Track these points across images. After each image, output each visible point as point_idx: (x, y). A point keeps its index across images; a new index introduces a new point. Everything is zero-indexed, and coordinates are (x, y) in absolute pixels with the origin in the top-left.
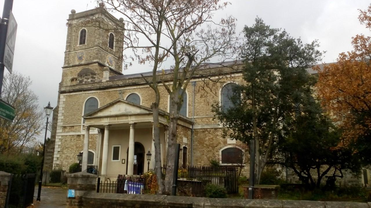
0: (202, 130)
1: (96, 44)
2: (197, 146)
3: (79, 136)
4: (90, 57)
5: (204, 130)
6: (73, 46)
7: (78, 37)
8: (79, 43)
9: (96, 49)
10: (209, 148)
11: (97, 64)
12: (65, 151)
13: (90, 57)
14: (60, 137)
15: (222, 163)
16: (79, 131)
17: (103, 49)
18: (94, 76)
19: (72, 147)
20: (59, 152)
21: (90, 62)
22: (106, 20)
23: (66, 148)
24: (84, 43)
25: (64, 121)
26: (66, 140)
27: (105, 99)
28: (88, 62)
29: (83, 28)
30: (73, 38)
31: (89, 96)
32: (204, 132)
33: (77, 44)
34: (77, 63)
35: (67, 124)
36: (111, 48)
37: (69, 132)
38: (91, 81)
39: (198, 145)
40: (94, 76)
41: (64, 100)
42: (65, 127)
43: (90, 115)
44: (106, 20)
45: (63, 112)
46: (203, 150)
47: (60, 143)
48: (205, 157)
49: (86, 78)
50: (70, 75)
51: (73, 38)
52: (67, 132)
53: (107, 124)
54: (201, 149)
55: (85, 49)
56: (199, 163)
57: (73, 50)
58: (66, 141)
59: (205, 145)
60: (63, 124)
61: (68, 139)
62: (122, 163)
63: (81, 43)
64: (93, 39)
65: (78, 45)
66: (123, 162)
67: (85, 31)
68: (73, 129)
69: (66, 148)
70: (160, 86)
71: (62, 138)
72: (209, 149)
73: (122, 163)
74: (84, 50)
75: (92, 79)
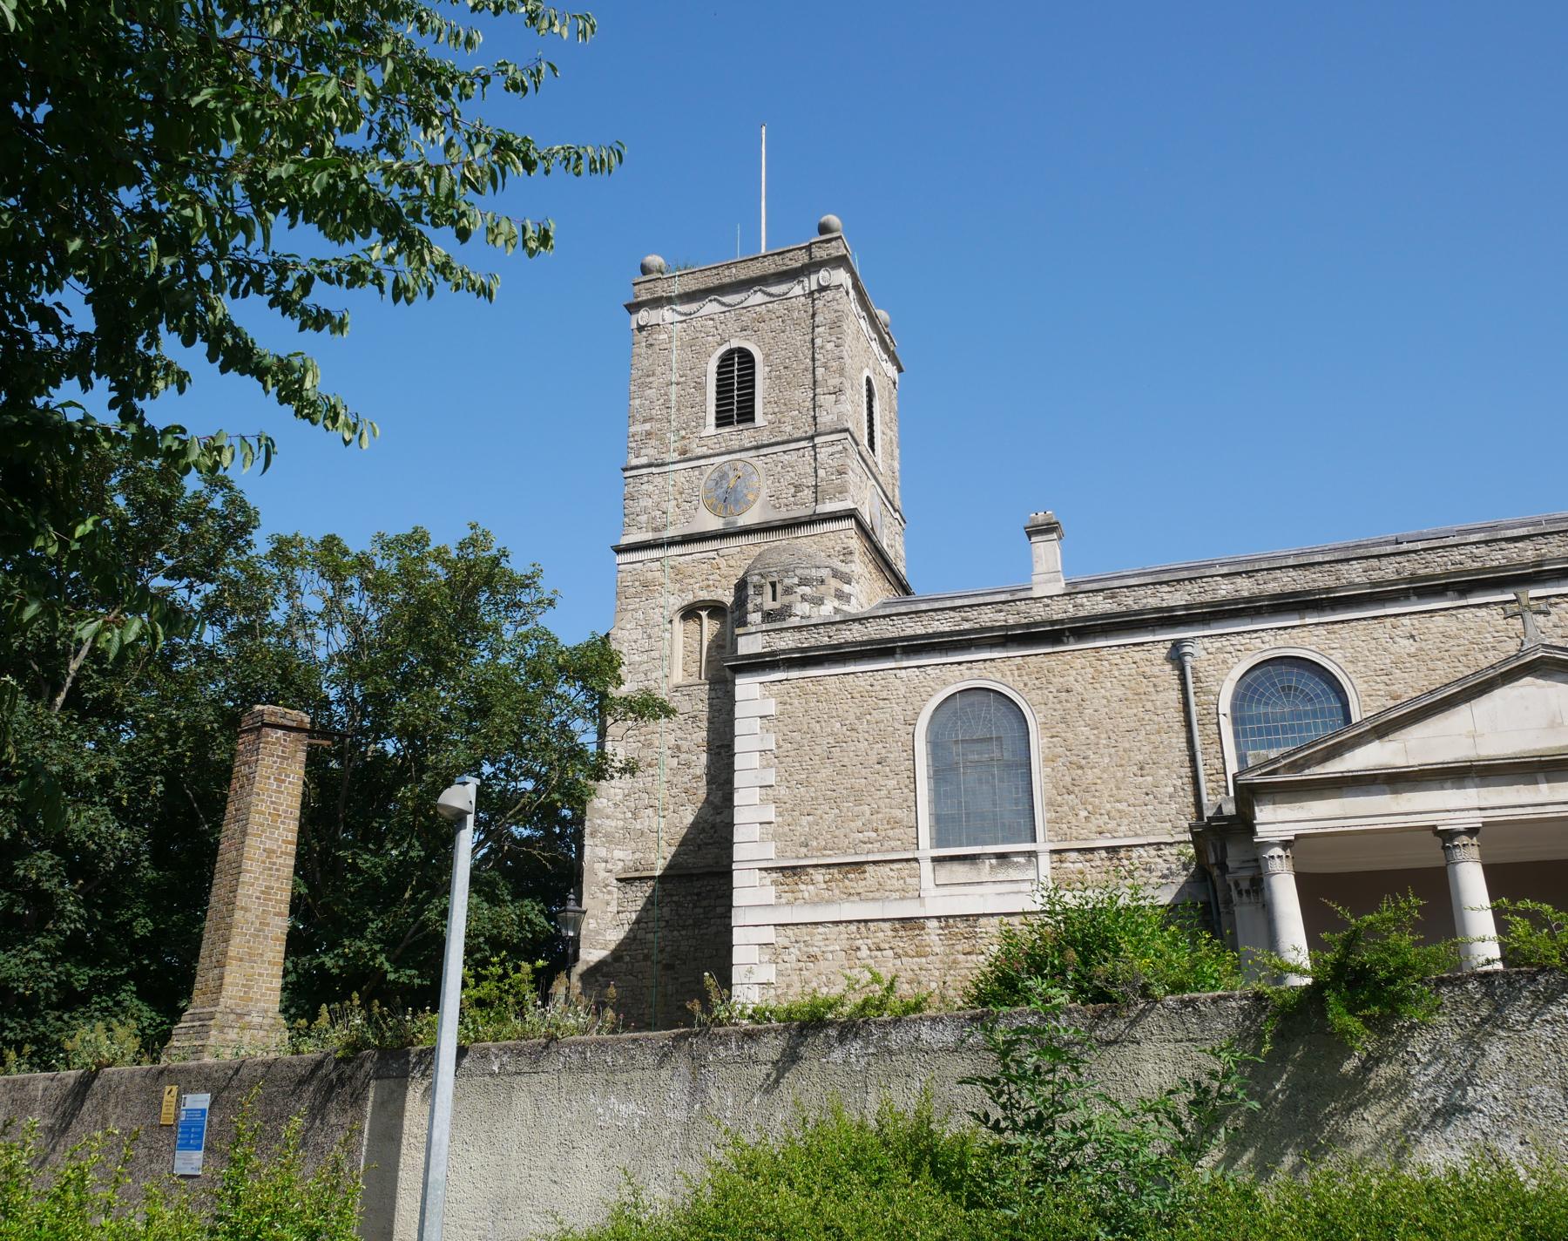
3: (909, 923)
4: (798, 488)
7: (700, 386)
8: (711, 418)
9: (832, 443)
11: (851, 523)
13: (798, 488)
14: (769, 935)
18: (846, 588)
24: (747, 415)
25: (775, 837)
26: (813, 950)
27: (1075, 699)
29: (735, 344)
30: (673, 397)
31: (945, 683)
33: (700, 421)
34: (714, 523)
35: (804, 850)
37: (829, 902)
38: (837, 610)
40: (846, 588)
41: (771, 707)
45: (771, 777)
49: (804, 598)
50: (670, 586)
51: (673, 397)
53: (1475, 820)
55: (757, 448)
57: (675, 456)
58: (812, 958)
60: (781, 854)
61: (837, 941)
63: (723, 420)
65: (711, 429)
67: (746, 357)
68: (854, 882)
70: (1479, 606)
71: (784, 942)
74: (752, 453)
75: (836, 603)
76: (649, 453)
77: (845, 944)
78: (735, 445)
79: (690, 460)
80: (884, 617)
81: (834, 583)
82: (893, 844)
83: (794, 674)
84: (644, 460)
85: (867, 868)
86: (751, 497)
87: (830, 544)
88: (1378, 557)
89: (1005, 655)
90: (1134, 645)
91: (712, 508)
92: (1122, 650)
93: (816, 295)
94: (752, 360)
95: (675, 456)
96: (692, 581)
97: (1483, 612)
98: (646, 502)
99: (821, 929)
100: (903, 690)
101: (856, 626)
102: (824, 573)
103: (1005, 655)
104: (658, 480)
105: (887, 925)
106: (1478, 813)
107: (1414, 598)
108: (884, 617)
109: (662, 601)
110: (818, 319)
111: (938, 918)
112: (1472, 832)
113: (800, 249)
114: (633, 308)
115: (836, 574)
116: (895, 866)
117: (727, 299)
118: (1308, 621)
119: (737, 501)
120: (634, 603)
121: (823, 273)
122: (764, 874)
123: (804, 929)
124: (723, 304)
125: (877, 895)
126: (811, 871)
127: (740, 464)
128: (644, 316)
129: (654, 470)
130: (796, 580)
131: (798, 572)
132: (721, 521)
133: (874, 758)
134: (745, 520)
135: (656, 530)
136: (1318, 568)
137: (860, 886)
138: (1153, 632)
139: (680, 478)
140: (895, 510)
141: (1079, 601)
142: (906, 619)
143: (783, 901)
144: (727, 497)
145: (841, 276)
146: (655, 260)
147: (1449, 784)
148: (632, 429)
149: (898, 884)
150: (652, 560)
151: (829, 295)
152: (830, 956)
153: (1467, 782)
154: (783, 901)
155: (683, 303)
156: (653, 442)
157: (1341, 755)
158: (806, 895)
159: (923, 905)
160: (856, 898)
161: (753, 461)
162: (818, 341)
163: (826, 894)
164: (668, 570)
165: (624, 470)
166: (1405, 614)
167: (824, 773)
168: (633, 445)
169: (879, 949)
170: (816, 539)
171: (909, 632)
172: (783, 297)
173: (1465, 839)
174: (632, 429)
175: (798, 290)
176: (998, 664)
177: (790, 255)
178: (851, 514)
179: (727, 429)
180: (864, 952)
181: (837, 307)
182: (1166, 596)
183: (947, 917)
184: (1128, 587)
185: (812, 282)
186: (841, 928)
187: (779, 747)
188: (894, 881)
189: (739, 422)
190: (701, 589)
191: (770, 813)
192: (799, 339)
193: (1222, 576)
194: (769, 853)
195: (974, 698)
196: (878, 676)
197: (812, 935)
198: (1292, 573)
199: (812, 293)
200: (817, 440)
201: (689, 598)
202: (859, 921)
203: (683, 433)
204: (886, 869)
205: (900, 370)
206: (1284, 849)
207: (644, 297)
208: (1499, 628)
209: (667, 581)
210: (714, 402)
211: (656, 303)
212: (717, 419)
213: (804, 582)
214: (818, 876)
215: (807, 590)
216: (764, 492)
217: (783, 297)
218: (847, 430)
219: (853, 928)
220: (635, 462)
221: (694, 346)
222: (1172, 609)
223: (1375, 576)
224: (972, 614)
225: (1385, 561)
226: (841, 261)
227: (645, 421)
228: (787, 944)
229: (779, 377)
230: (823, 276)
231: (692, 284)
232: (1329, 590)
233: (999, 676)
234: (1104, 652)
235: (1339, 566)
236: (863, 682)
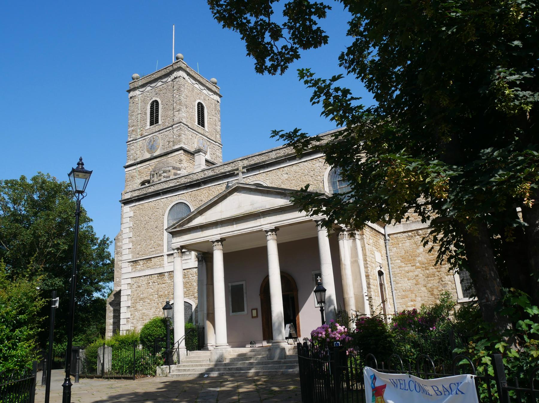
0: (406, 234)
1: (176, 120)
2: (400, 267)
3: (161, 274)
4: (169, 142)
5: (410, 234)
6: (139, 130)
7: (146, 114)
8: (148, 123)
10: (428, 269)
11: (182, 151)
12: (139, 306)
13: (169, 142)
14: (129, 281)
15: (464, 297)
16: (161, 266)
17: (189, 127)
19: (152, 297)
20: (128, 307)
21: (169, 150)
22: (189, 81)
23: (142, 299)
24: (157, 122)
25: (132, 252)
28: (165, 151)
29: (154, 99)
31: (172, 202)
32: (412, 237)
34: (148, 156)
36: (202, 126)
37: (143, 270)
39: (404, 265)
41: (132, 214)
42: (135, 262)
43: (180, 226)
44: (189, 81)
45: (131, 235)
46: (416, 273)
47: (129, 292)
48: (424, 289)
50: (138, 177)
51: (139, 118)
52: (139, 271)
53: (218, 237)
54: (411, 274)
55: (159, 131)
56: (412, 303)
58: (139, 287)
59: (418, 264)
60: (133, 257)
62: (253, 317)
63: (152, 124)
64: (170, 113)
65: (148, 126)
66: (254, 312)
68: (150, 264)
69: (142, 299)
72: (428, 272)
73: (253, 317)
74: (158, 133)
76: (133, 136)
77: (146, 282)
78: (154, 131)
79: (143, 137)
80: (159, 183)
81: (173, 171)
82: (158, 251)
83: (137, 203)
84: (132, 139)
85: (152, 259)
86: (157, 147)
87: (176, 159)
88: (279, 149)
89: (186, 192)
90: (218, 184)
91: (148, 151)
92: (215, 186)
93: (174, 80)
94: (158, 104)
95: (139, 136)
96: (143, 174)
97: (305, 164)
98: (132, 152)
99: (141, 278)
100: (162, 205)
101: (152, 187)
102: (170, 168)
103: (186, 192)
104: (135, 144)
105: (156, 275)
106: (219, 235)
107: (288, 161)
108: (159, 183)
109: (136, 182)
110: (175, 88)
111: (168, 272)
112: (217, 241)
113: (170, 66)
114: (129, 91)
115: (174, 168)
116: (159, 258)
117: (152, 85)
118: (261, 172)
119: (154, 148)
120: (129, 183)
121: (175, 73)
122: (129, 263)
123: (138, 279)
124: (151, 87)
125: (154, 267)
126: (139, 261)
127: (155, 137)
128: (132, 94)
129: (134, 141)
130: (162, 172)
131: (163, 169)
132: (150, 155)
133: (155, 226)
134: (155, 154)
135: (135, 160)
136: (264, 155)
137: (150, 265)
138: (223, 180)
139: (140, 143)
140: (216, 142)
141: (205, 173)
142: (164, 183)
143: (133, 271)
144: (151, 148)
145: (181, 73)
146: (136, 75)
147: (214, 227)
148: (129, 130)
149: (159, 263)
150: (134, 169)
151: (177, 80)
152: (143, 286)
153: (218, 226)
154: (133, 271)
155: (141, 88)
156: (134, 133)
157: (192, 221)
158: (138, 268)
159: (164, 269)
160: (149, 268)
161: (158, 135)
162: (174, 95)
163: (143, 268)
164: (137, 172)
165: (127, 142)
166: (285, 167)
167: (143, 232)
168: (129, 134)
169: (154, 283)
170: (173, 157)
171: (165, 187)
172: (166, 82)
173: (216, 243)
174: (129, 130)
175: (170, 80)
176: (185, 194)
177: (168, 68)
178: (181, 149)
179: (152, 126)
180: (151, 284)
181: (179, 83)
182: (226, 168)
183: (170, 272)
184: (217, 167)
185: (172, 77)
186: (146, 277)
187: (133, 226)
188: (158, 263)
189: (155, 123)
190: (145, 176)
191: (130, 246)
192: (170, 95)
193: (240, 160)
194: (130, 257)
195: (180, 205)
196: (157, 201)
197: (139, 280)
198: (258, 157)
199: (173, 80)
200: (174, 126)
201: (143, 180)
202: (150, 275)
203: (141, 129)
204: (156, 259)
205: (220, 96)
206: (178, 250)
207: (132, 87)
208: (309, 168)
209: (137, 175)
210: (149, 118)
211: (135, 89)
212: (150, 123)
213: (164, 172)
214: (141, 263)
215: (165, 174)
216: (161, 145)
217: (166, 82)
218: (181, 122)
219: (148, 277)
220: (130, 140)
221: (144, 101)
222: (225, 173)
223: (278, 155)
224: (179, 180)
225: (281, 150)
226: (180, 69)
227: (132, 127)
228: (134, 283)
229: (165, 108)
230: (175, 74)
231: (144, 81)
232: (264, 162)
233: (185, 198)
234: (211, 188)
235: (269, 154)
236: (152, 204)
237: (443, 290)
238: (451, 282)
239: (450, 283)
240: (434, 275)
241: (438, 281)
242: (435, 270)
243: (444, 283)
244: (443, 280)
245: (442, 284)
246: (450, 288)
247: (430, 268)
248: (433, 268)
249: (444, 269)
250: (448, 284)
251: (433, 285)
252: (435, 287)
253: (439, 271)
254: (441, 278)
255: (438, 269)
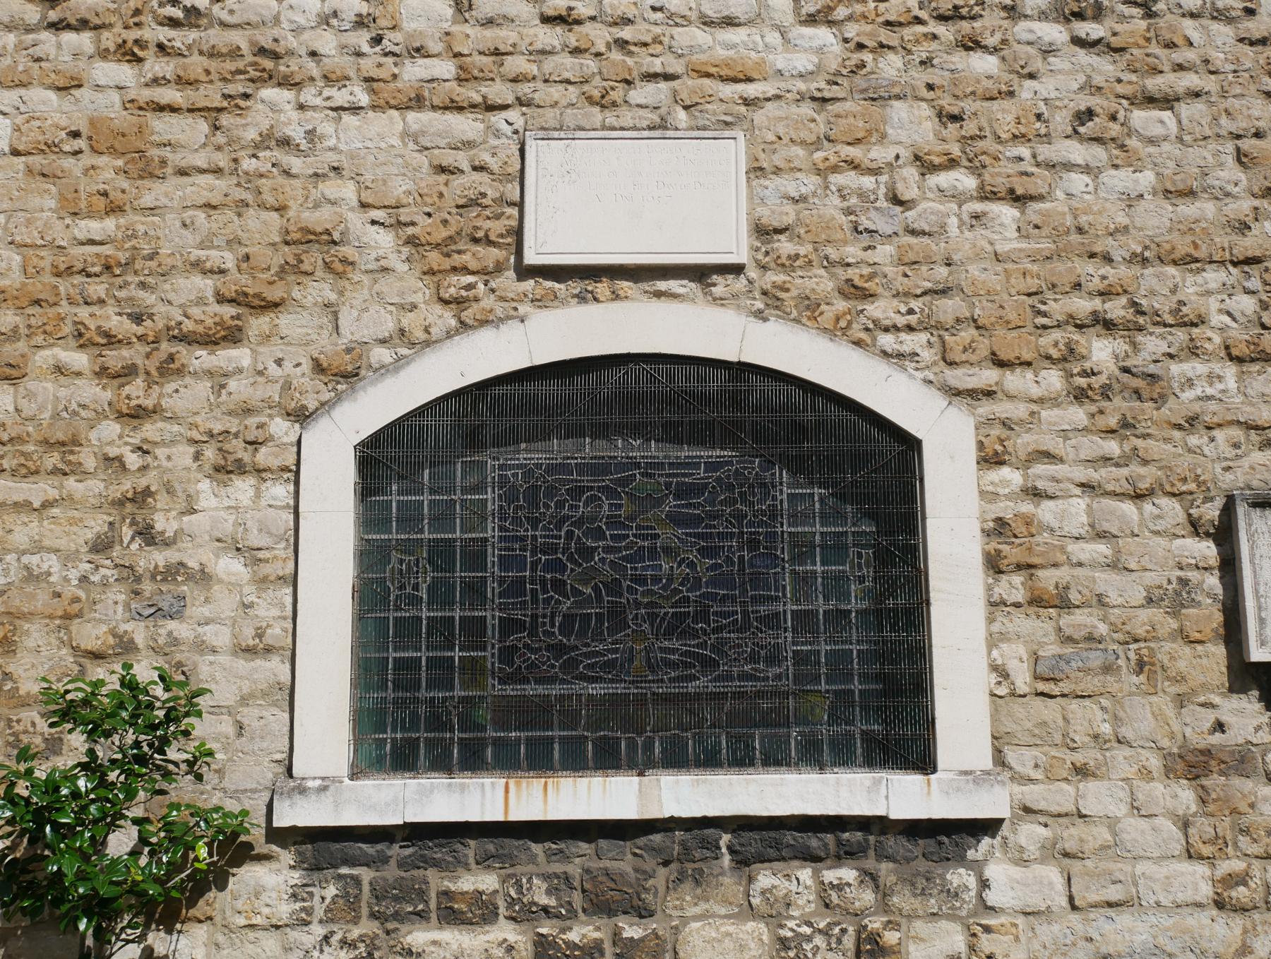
237: (126, 646)
238: (251, 555)
239: (230, 567)
240: (70, 444)
241: (97, 524)
242: (93, 392)
243: (160, 558)
244: (164, 523)
245: (129, 574)
246: (220, 636)
247: (44, 358)
248: (80, 360)
249: (203, 388)
250: (203, 577)
251: (31, 576)
252: (42, 599)
253: (137, 415)
254: (142, 497)
255: (135, 389)
